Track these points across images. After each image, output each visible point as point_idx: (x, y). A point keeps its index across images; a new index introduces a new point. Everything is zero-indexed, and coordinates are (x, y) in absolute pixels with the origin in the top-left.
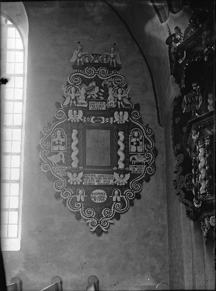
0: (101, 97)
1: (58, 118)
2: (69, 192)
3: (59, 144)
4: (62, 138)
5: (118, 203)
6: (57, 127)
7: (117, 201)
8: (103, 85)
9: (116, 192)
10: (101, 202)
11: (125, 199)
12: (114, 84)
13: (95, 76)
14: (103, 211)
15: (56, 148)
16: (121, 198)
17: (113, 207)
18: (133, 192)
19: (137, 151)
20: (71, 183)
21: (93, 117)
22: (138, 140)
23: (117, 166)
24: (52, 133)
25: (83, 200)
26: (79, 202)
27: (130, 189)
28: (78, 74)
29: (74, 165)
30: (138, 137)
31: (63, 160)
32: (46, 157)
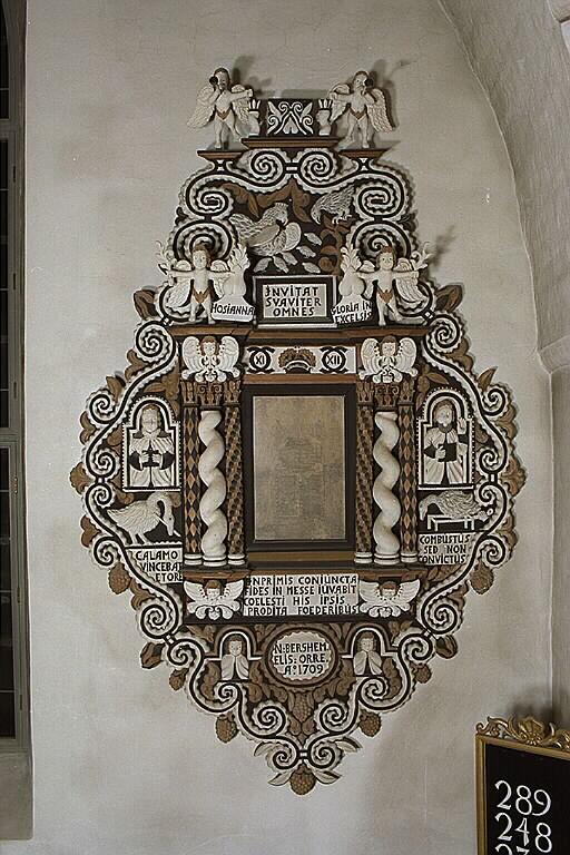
0: (307, 266)
1: (145, 358)
2: (192, 646)
3: (150, 464)
4: (163, 435)
5: (372, 681)
6: (141, 394)
7: (367, 671)
8: (315, 215)
9: (367, 644)
10: (309, 676)
11: (399, 666)
12: (359, 211)
13: (284, 182)
14: (318, 712)
15: (139, 479)
16: (383, 659)
17: (353, 695)
18: (427, 639)
19: (445, 482)
20: (201, 616)
21: (280, 350)
22: (452, 438)
23: (372, 548)
24: (126, 420)
25: (243, 674)
26: (229, 682)
27: (420, 626)
28: (218, 177)
29: (212, 547)
30: (454, 425)
31: (169, 524)
32: (104, 513)
